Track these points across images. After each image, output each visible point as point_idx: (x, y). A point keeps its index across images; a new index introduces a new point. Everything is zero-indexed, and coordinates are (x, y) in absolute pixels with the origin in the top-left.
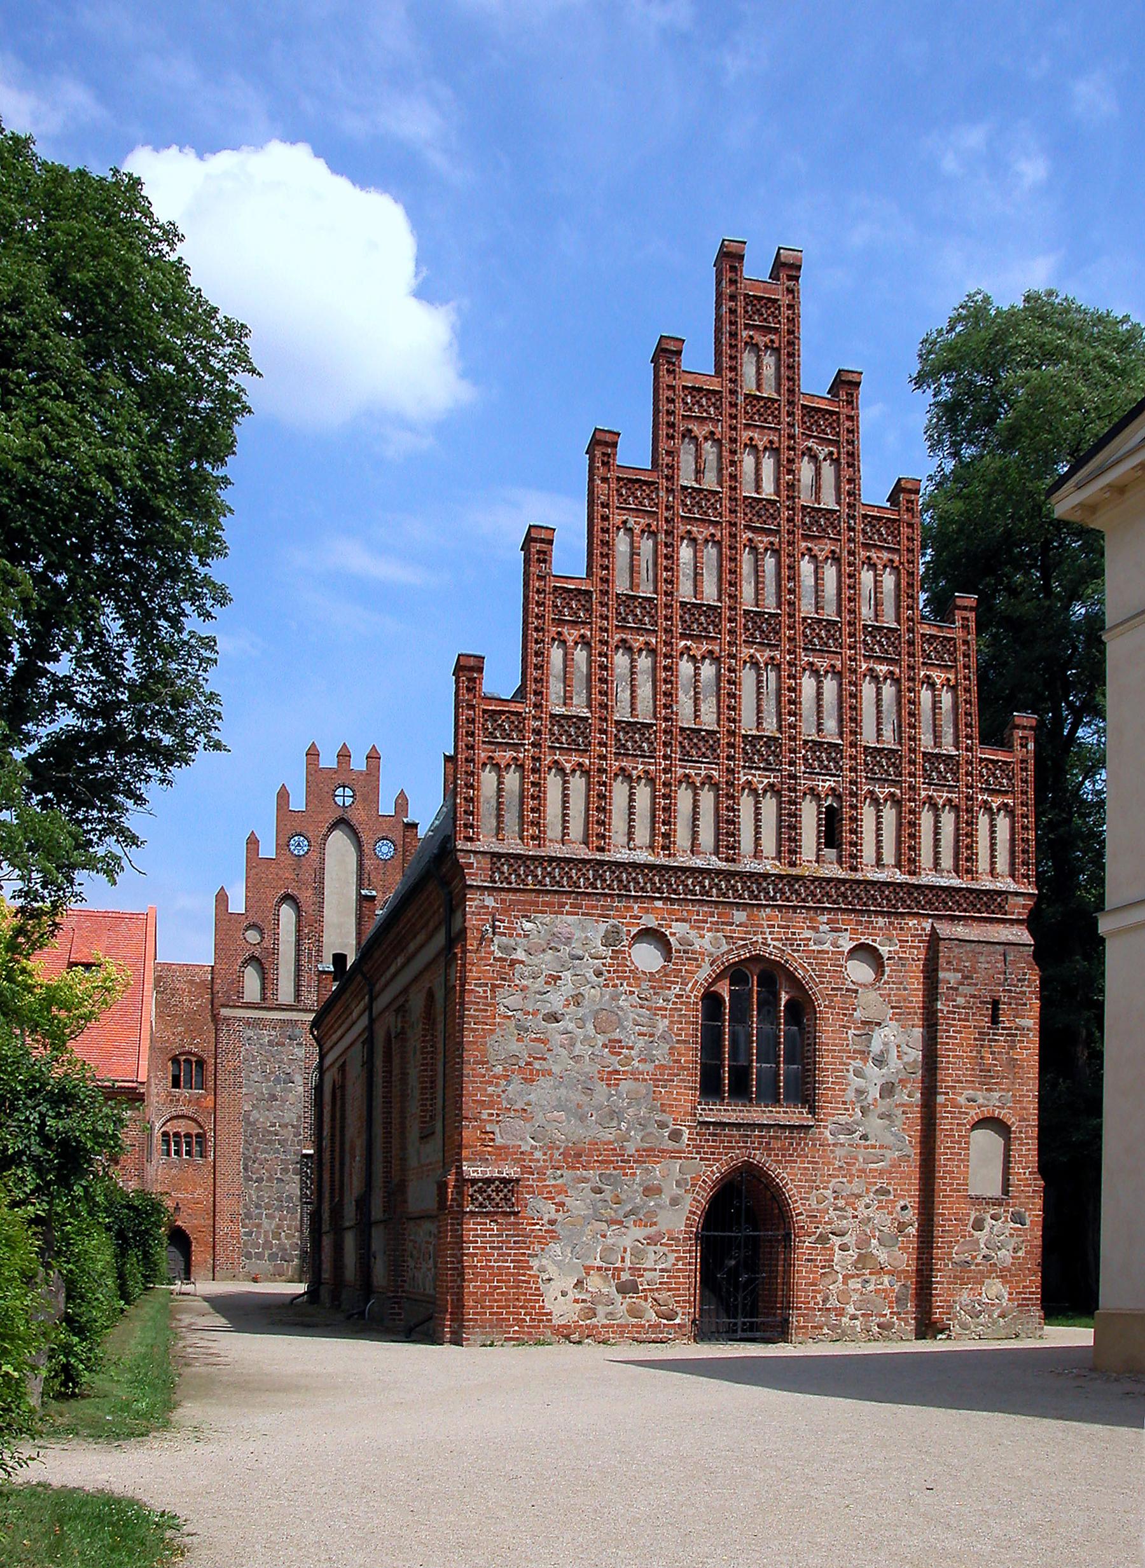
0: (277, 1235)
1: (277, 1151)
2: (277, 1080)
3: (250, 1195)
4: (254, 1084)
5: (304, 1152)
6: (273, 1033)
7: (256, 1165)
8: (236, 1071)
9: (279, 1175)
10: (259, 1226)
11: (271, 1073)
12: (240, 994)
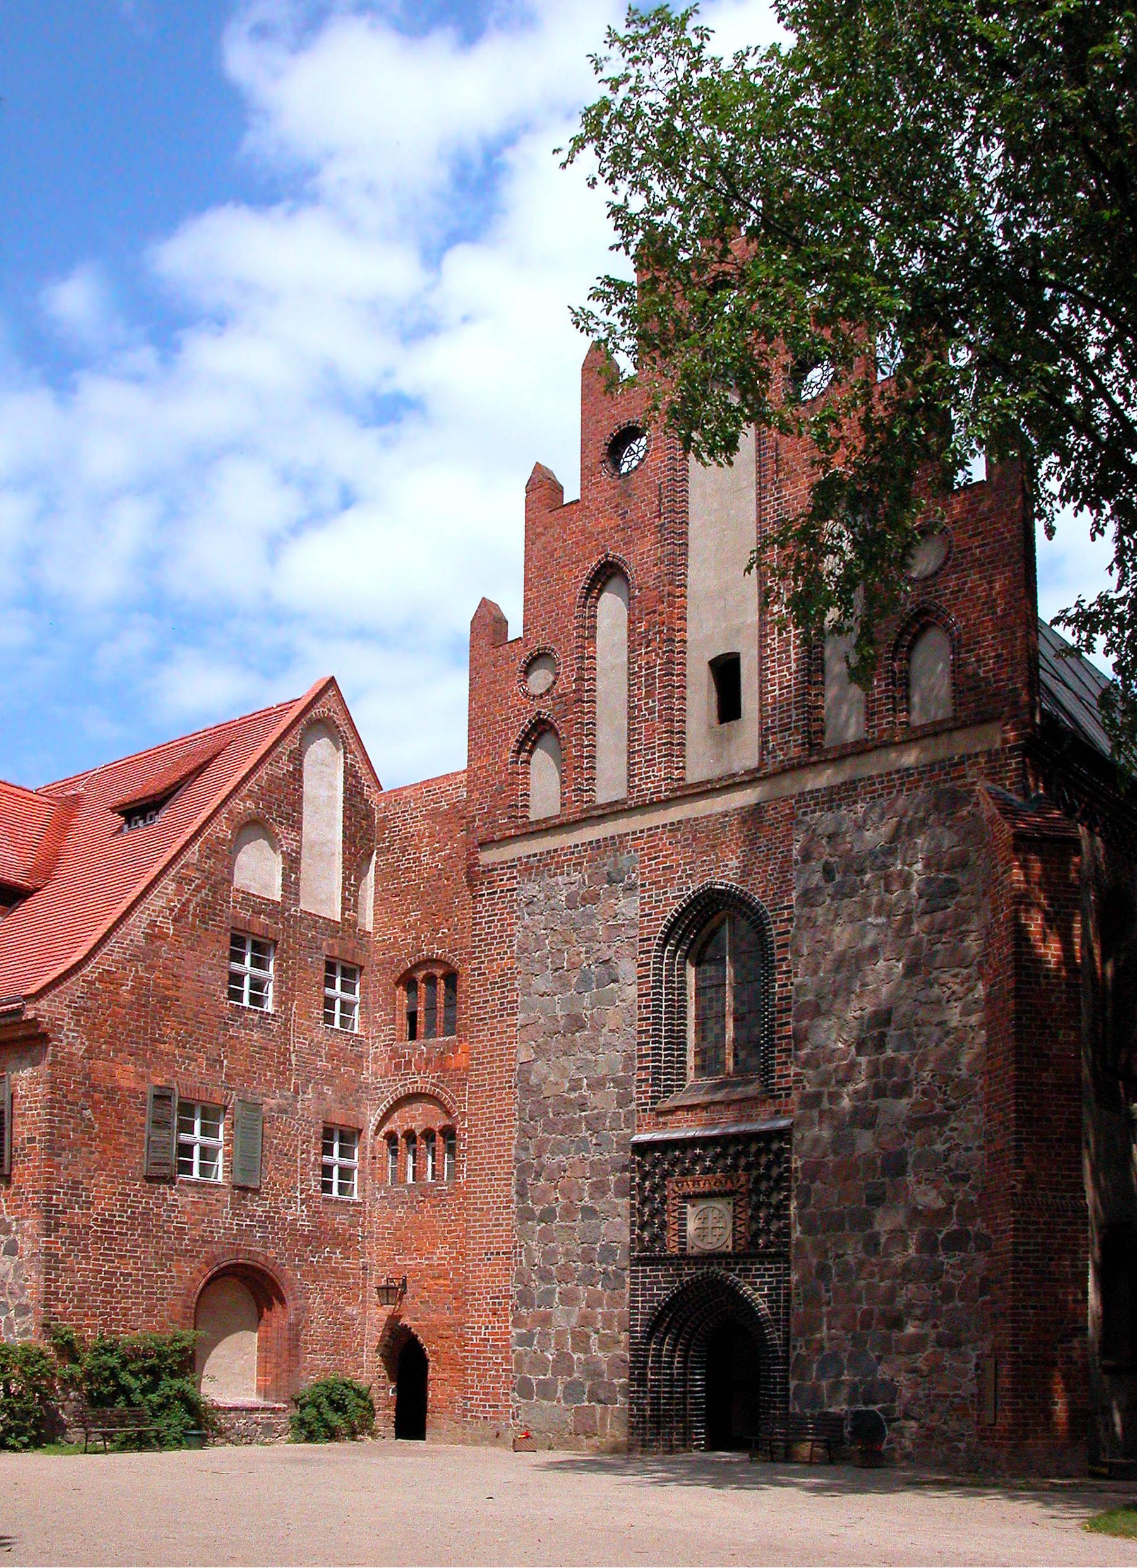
0: (581, 1341)
1: (583, 1145)
2: (585, 982)
3: (529, 1250)
4: (541, 998)
5: (635, 1138)
6: (576, 876)
8: (506, 977)
9: (587, 1201)
10: (546, 1320)
11: (573, 966)
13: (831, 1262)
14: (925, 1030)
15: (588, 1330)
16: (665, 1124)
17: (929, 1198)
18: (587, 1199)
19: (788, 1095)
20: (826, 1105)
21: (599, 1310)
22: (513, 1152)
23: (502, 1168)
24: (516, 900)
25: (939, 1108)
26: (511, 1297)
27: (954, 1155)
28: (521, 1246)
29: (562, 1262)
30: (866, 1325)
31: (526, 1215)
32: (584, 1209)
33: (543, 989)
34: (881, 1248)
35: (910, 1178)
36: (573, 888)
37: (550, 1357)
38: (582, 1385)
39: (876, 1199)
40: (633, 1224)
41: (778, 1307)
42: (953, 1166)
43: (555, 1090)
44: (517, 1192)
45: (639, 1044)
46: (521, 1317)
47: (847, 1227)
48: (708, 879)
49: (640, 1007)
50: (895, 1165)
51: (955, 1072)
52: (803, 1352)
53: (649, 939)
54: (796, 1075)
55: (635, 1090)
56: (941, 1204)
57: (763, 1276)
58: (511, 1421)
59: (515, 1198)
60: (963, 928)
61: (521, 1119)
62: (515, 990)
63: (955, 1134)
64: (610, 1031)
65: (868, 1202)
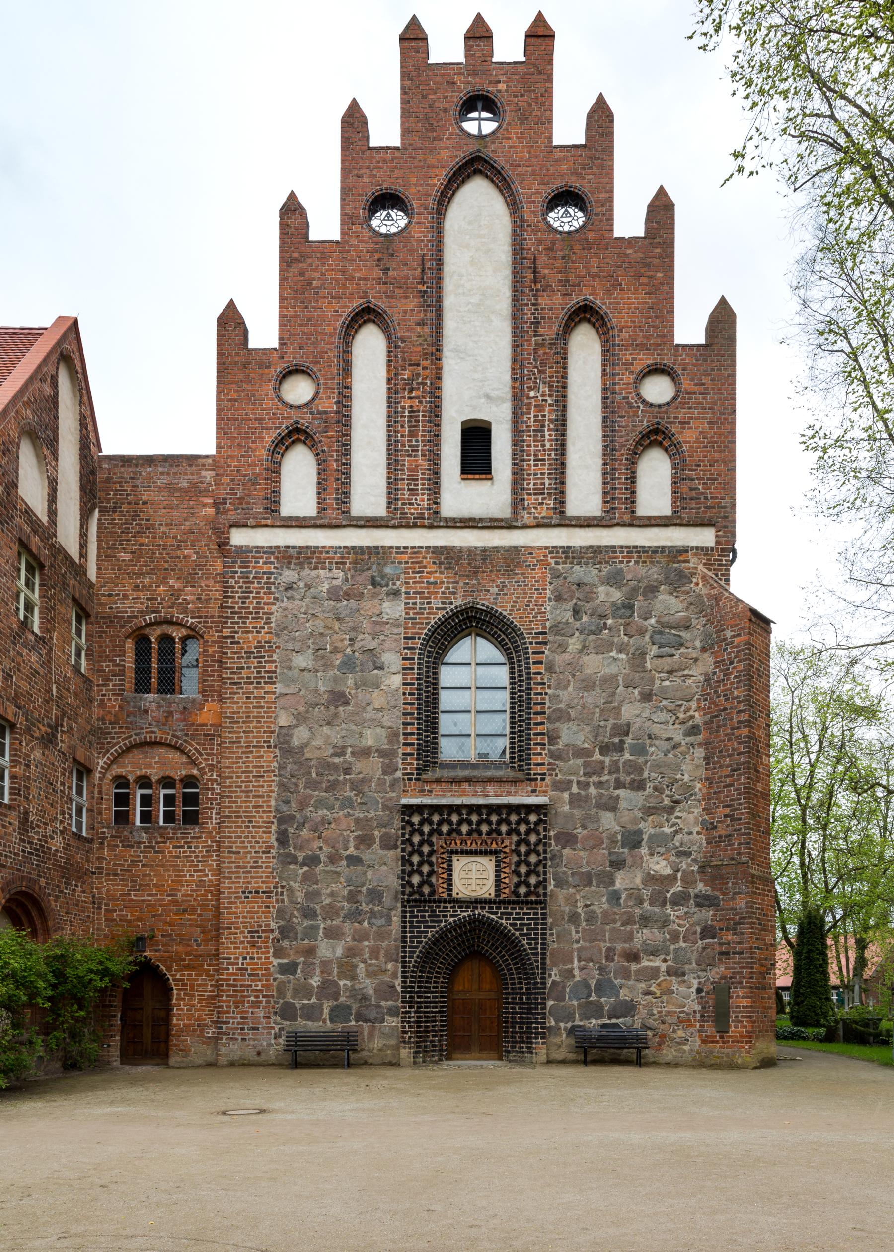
1: (347, 803)
2: (348, 665)
3: (291, 891)
5: (404, 801)
7: (305, 833)
8: (262, 650)
9: (351, 850)
10: (310, 952)
11: (335, 651)
12: (273, 502)
13: (579, 910)
14: (657, 742)
15: (355, 960)
16: (430, 792)
17: (661, 866)
18: (352, 849)
19: (543, 779)
20: (575, 789)
21: (366, 943)
22: (273, 803)
23: (261, 817)
24: (274, 583)
25: (667, 802)
26: (272, 931)
27: (679, 837)
28: (283, 887)
29: (327, 901)
30: (609, 959)
31: (288, 860)
32: (349, 858)
33: (303, 665)
34: (622, 901)
35: (644, 850)
36: (335, 582)
37: (315, 984)
38: (349, 1007)
39: (618, 864)
40: (403, 872)
41: (537, 944)
42: (678, 844)
43: (318, 754)
44: (277, 839)
45: (404, 724)
46: (282, 949)
47: (594, 883)
48: (470, 599)
49: (404, 694)
50: (633, 840)
51: (679, 776)
52: (558, 979)
53: (414, 638)
54: (549, 764)
55: (400, 761)
56: (668, 871)
57: (523, 919)
58: (273, 1042)
59: (276, 844)
60: (686, 672)
61: (280, 775)
62: (274, 661)
63: (679, 821)
64: (375, 709)
65: (611, 866)
